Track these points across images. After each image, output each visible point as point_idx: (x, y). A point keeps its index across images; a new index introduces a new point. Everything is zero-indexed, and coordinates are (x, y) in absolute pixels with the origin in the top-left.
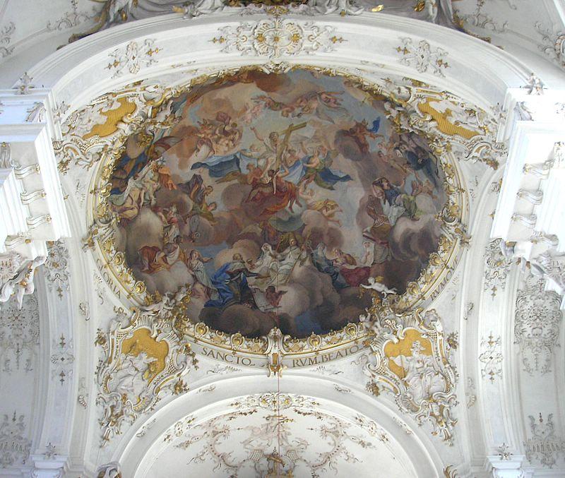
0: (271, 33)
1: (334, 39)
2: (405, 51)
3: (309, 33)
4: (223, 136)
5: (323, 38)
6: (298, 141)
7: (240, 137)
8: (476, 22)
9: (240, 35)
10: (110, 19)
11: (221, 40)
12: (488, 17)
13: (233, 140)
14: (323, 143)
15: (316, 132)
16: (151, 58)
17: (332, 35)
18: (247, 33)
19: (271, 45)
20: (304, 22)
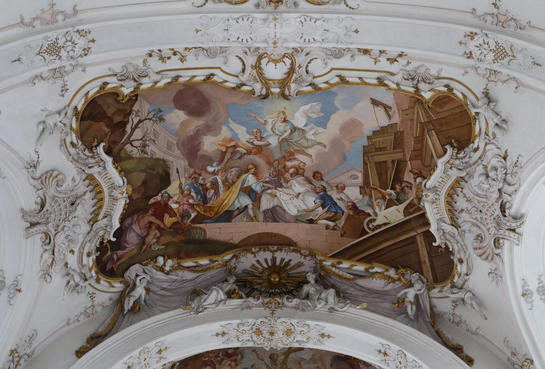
0: (268, 329)
1: (323, 335)
2: (385, 354)
3: (301, 329)
4: (226, 358)
5: (314, 334)
6: (296, 361)
7: (242, 357)
8: (452, 320)
9: (240, 330)
10: (125, 310)
11: (224, 334)
12: (462, 318)
13: (235, 361)
14: (319, 365)
15: (313, 355)
16: (161, 356)
17: (322, 332)
18: (246, 328)
19: (267, 337)
20: (296, 321)
